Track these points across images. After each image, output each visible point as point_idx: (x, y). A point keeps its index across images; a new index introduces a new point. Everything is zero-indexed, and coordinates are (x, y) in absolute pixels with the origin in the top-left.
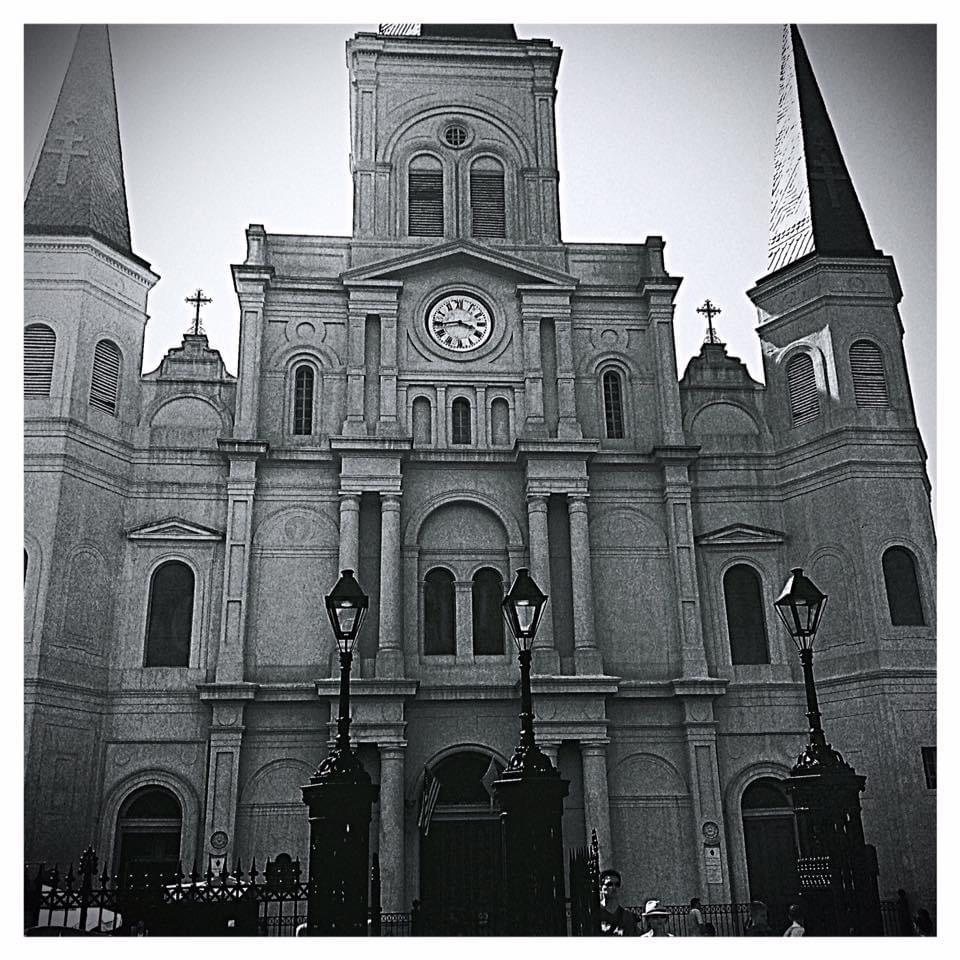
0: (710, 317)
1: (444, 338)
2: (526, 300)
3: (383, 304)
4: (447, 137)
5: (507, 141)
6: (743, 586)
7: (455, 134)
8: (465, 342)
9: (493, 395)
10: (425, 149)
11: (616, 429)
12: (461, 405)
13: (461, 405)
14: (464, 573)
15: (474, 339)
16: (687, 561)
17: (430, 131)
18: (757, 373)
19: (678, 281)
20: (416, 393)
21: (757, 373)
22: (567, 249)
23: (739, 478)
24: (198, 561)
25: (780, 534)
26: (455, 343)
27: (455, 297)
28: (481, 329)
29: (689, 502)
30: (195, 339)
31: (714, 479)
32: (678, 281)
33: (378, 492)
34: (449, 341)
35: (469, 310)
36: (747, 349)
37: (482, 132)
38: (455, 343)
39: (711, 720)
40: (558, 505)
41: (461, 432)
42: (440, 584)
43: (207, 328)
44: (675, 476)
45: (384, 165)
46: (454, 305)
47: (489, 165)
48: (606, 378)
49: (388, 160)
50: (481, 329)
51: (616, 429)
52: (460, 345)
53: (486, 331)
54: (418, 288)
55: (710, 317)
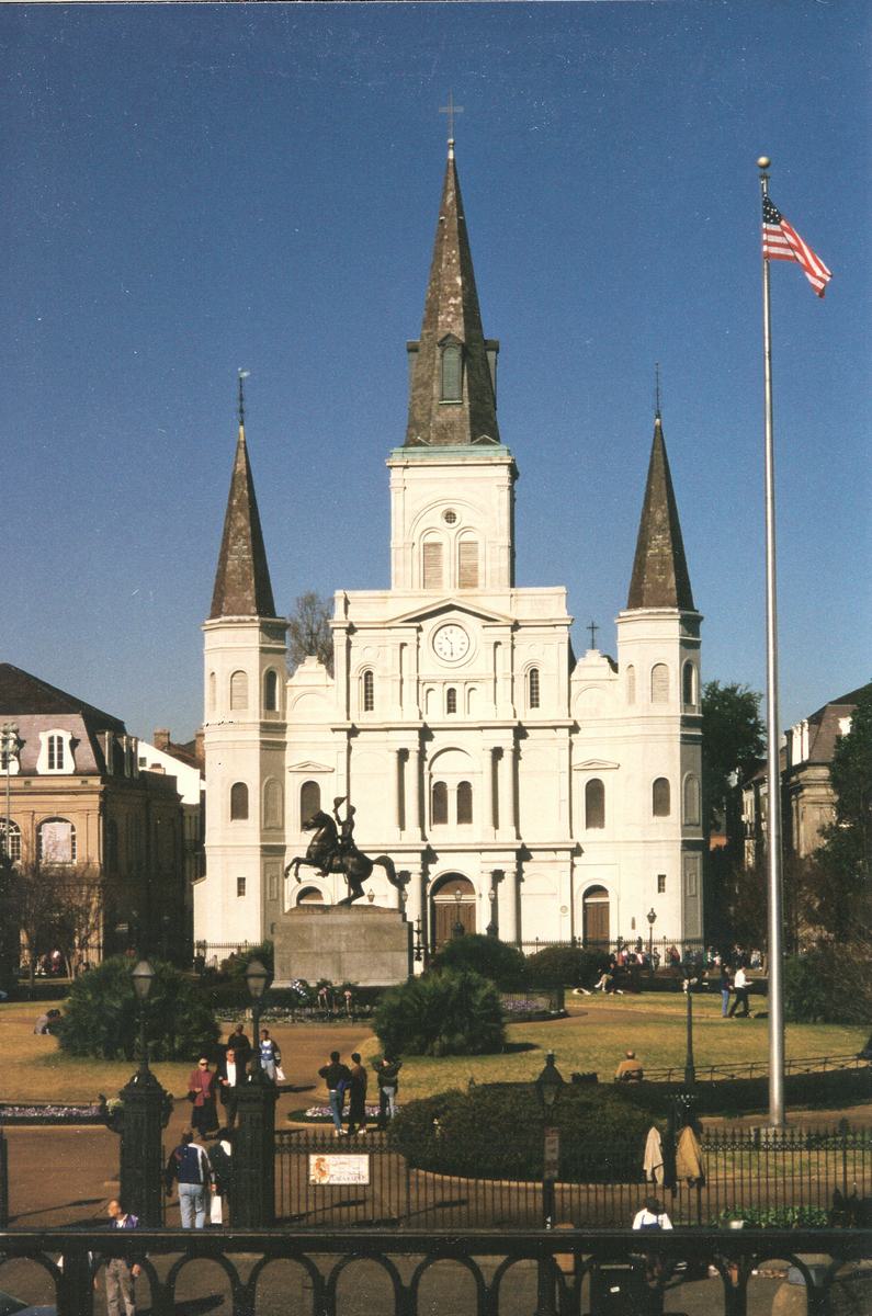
3: (409, 635)
6: (595, 791)
7: (450, 517)
9: (470, 686)
10: (430, 530)
11: (534, 703)
12: (451, 692)
13: (451, 692)
20: (427, 686)
27: (449, 627)
35: (456, 635)
37: (463, 517)
41: (451, 708)
42: (440, 790)
47: (467, 537)
48: (532, 671)
49: (411, 541)
51: (534, 703)
54: (428, 625)
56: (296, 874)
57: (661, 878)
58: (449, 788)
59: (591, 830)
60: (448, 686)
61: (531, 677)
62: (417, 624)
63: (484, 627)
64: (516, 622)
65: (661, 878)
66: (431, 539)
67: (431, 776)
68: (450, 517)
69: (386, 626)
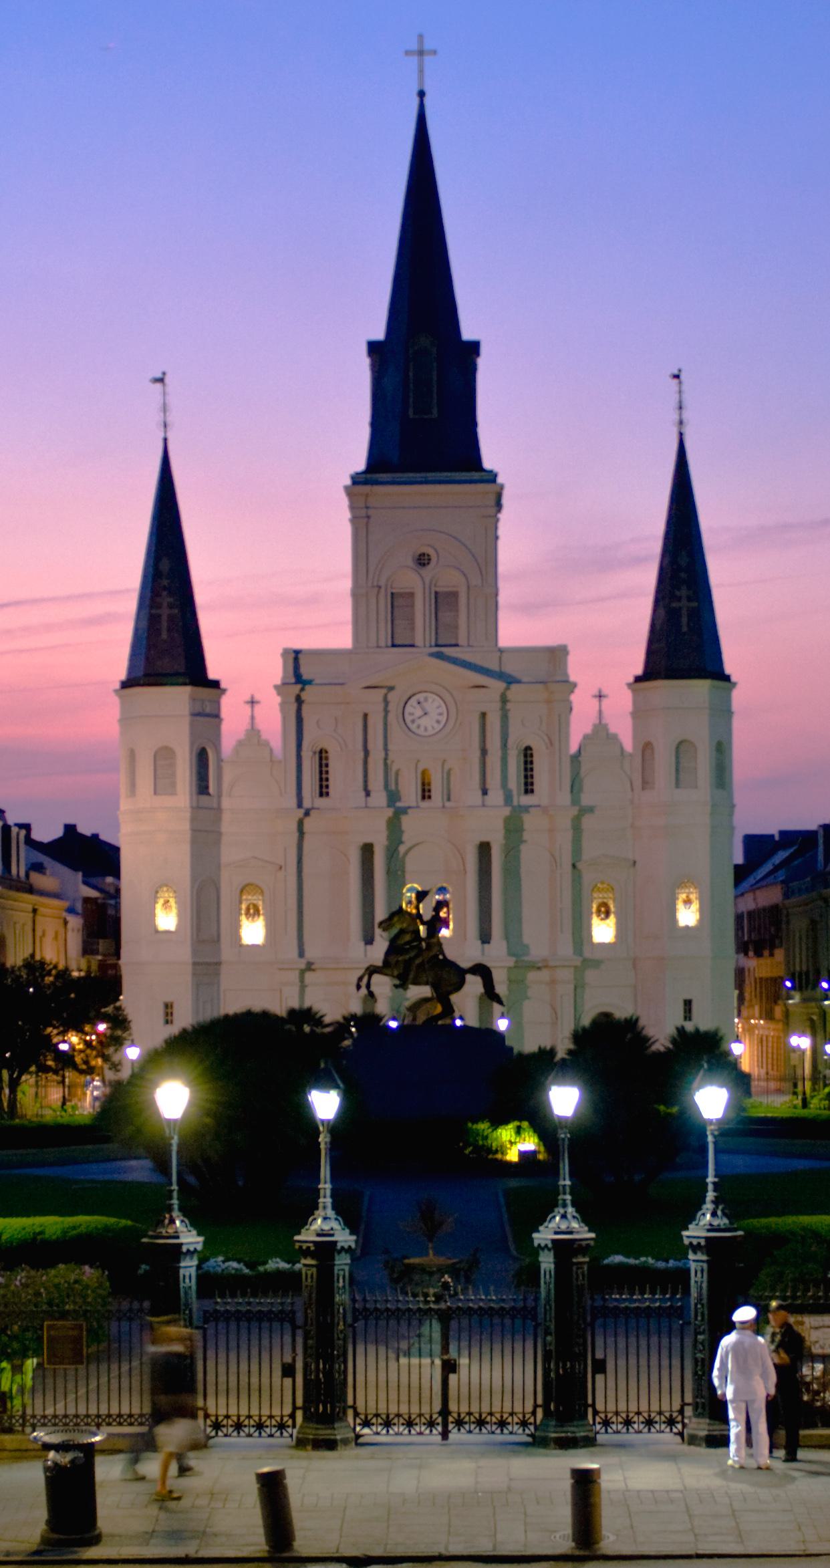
0: (600, 701)
8: (430, 728)
15: (436, 725)
18: (628, 746)
19: (575, 685)
21: (628, 746)
22: (501, 651)
26: (422, 729)
28: (440, 718)
30: (253, 731)
32: (575, 685)
36: (623, 729)
38: (422, 729)
43: (260, 725)
50: (440, 718)
53: (443, 719)
56: (368, 986)
61: (525, 756)
65: (688, 1004)
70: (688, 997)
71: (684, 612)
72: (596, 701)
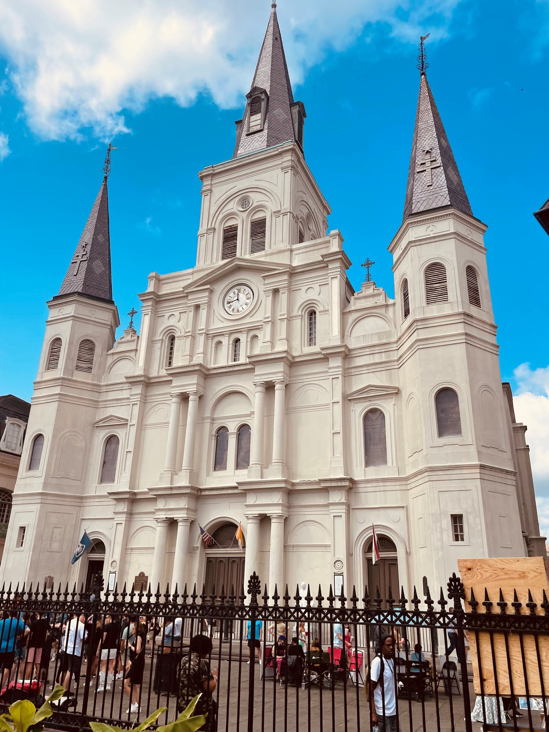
1: (231, 309)
2: (267, 281)
3: (202, 298)
4: (242, 206)
5: (266, 198)
7: (244, 202)
8: (240, 309)
9: (252, 333)
10: (231, 216)
14: (233, 427)
15: (245, 306)
16: (338, 408)
17: (233, 206)
23: (377, 359)
24: (121, 433)
25: (395, 388)
28: (248, 301)
29: (340, 376)
31: (359, 362)
33: (186, 392)
34: (233, 310)
37: (256, 199)
39: (343, 500)
40: (269, 387)
44: (336, 363)
45: (210, 229)
46: (236, 291)
47: (259, 216)
52: (238, 311)
54: (220, 288)
55: (368, 267)
57: (457, 519)
58: (229, 432)
59: (371, 469)
60: (234, 336)
62: (208, 286)
63: (264, 277)
64: (294, 268)
65: (457, 519)
66: (231, 223)
67: (213, 420)
68: (244, 202)
69: (184, 295)
70: (457, 512)
71: (429, 170)
72: (364, 269)
